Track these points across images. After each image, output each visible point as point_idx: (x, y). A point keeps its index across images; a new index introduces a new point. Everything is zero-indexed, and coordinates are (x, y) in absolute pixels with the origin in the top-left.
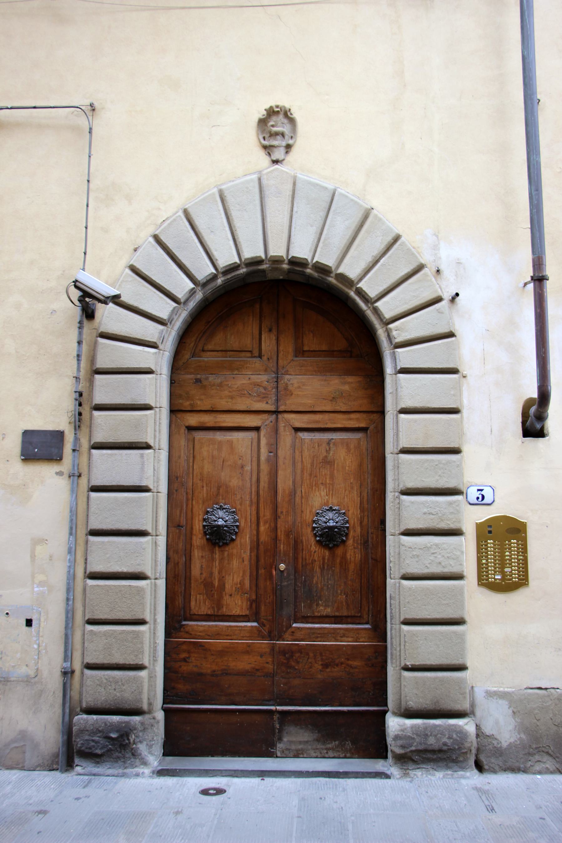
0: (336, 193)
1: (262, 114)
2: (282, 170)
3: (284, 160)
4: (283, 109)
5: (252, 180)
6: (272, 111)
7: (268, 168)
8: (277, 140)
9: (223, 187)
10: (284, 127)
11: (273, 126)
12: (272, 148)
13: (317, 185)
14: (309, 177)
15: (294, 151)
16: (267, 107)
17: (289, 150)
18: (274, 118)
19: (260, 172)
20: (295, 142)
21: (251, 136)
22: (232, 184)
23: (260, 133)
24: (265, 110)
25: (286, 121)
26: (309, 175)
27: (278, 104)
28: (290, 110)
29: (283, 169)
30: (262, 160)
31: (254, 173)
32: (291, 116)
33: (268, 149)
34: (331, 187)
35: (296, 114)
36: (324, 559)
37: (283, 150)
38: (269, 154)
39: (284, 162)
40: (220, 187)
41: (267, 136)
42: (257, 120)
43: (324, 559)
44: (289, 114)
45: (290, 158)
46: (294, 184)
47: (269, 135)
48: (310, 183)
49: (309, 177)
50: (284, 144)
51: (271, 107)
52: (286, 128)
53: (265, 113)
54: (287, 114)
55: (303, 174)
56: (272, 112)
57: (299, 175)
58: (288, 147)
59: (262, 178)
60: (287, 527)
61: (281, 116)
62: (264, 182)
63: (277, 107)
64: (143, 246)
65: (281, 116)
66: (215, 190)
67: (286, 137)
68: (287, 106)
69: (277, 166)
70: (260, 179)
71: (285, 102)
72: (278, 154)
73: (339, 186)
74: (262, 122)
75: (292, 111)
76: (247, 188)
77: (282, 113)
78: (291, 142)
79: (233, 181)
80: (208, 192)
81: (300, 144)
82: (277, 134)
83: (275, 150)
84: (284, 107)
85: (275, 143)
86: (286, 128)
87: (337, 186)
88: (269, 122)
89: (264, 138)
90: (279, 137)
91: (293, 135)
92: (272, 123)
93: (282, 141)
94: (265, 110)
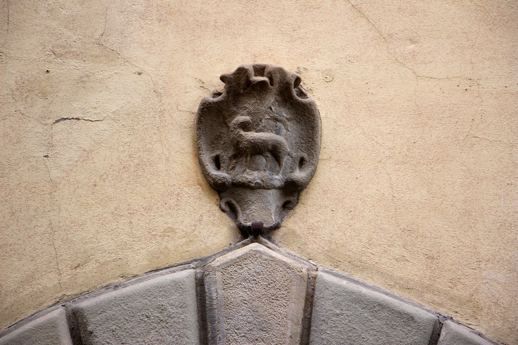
1: (213, 90)
3: (277, 227)
4: (277, 78)
5: (177, 285)
7: (228, 251)
8: (257, 169)
11: (245, 126)
12: (240, 191)
14: (357, 282)
16: (230, 69)
17: (291, 198)
18: (250, 104)
19: (202, 262)
20: (312, 175)
25: (284, 113)
26: (356, 277)
27: (260, 62)
28: (298, 80)
29: (274, 254)
31: (184, 265)
33: (228, 195)
35: (318, 94)
37: (273, 199)
38: (232, 211)
44: (294, 92)
49: (357, 282)
50: (278, 179)
51: (241, 71)
52: (285, 137)
53: (221, 86)
54: (288, 93)
55: (336, 270)
56: (242, 86)
58: (292, 193)
59: (207, 279)
61: (271, 99)
63: (260, 70)
65: (271, 99)
67: (286, 160)
68: (290, 69)
71: (284, 59)
74: (213, 117)
75: (304, 86)
77: (274, 89)
78: (299, 175)
82: (257, 149)
83: (251, 196)
84: (281, 71)
85: (253, 176)
86: (285, 137)
88: (234, 114)
89: (217, 162)
90: (262, 160)
91: (305, 155)
92: (241, 118)
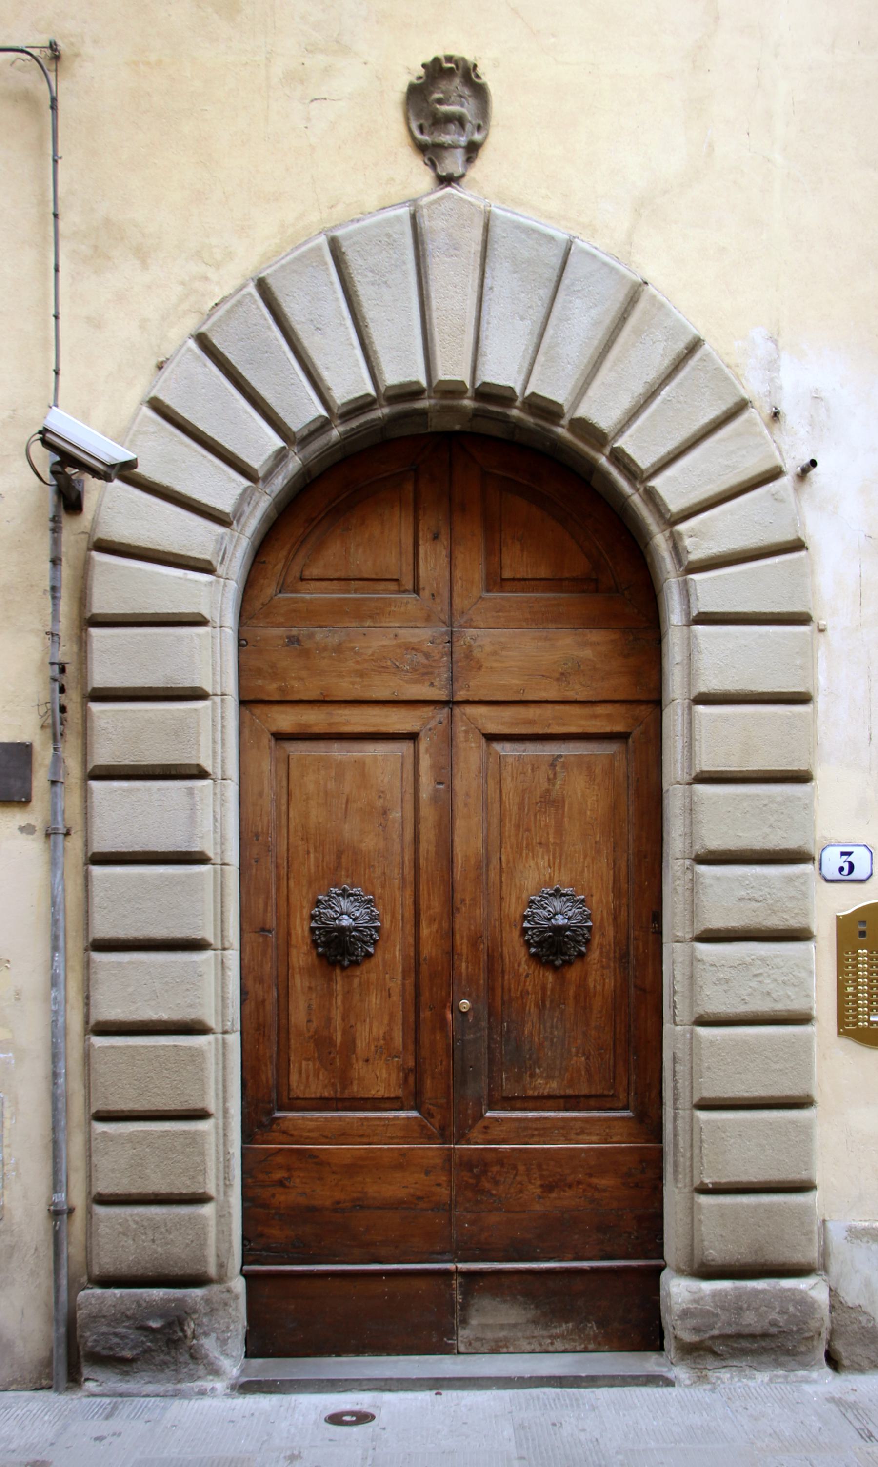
0: (573, 248)
1: (416, 74)
2: (461, 199)
3: (463, 176)
4: (461, 65)
5: (398, 219)
6: (437, 68)
8: (448, 133)
9: (338, 233)
10: (462, 106)
11: (440, 102)
13: (534, 231)
14: (517, 214)
15: (485, 155)
16: (429, 59)
17: (473, 155)
18: (443, 85)
19: (414, 202)
20: (486, 138)
21: (392, 125)
22: (356, 226)
23: (412, 118)
24: (424, 66)
25: (467, 92)
26: (516, 211)
28: (475, 66)
29: (462, 195)
30: (418, 177)
31: (402, 204)
32: (476, 80)
33: (430, 152)
34: (562, 236)
35: (488, 76)
37: (459, 155)
38: (433, 165)
39: (464, 181)
40: (331, 234)
41: (426, 124)
42: (405, 88)
45: (480, 171)
46: (487, 228)
47: (430, 122)
48: (518, 227)
49: (517, 214)
50: (463, 141)
51: (436, 60)
52: (467, 109)
53: (422, 72)
55: (503, 206)
56: (438, 71)
57: (493, 209)
58: (472, 150)
59: (417, 215)
60: (472, 928)
61: (457, 81)
62: (426, 223)
63: (449, 59)
64: (177, 360)
65: (457, 81)
66: (323, 240)
67: (468, 127)
68: (470, 58)
69: (448, 190)
70: (413, 217)
72: (453, 163)
73: (577, 234)
74: (418, 96)
75: (480, 71)
76: (388, 236)
77: (459, 73)
78: (477, 137)
79: (358, 221)
80: (306, 243)
81: (496, 141)
83: (446, 154)
84: (463, 59)
85: (446, 139)
86: (467, 109)
87: (574, 233)
88: (432, 93)
89: (421, 129)
90: (452, 127)
91: (481, 123)
92: (438, 95)
93: (460, 134)
94: (424, 66)
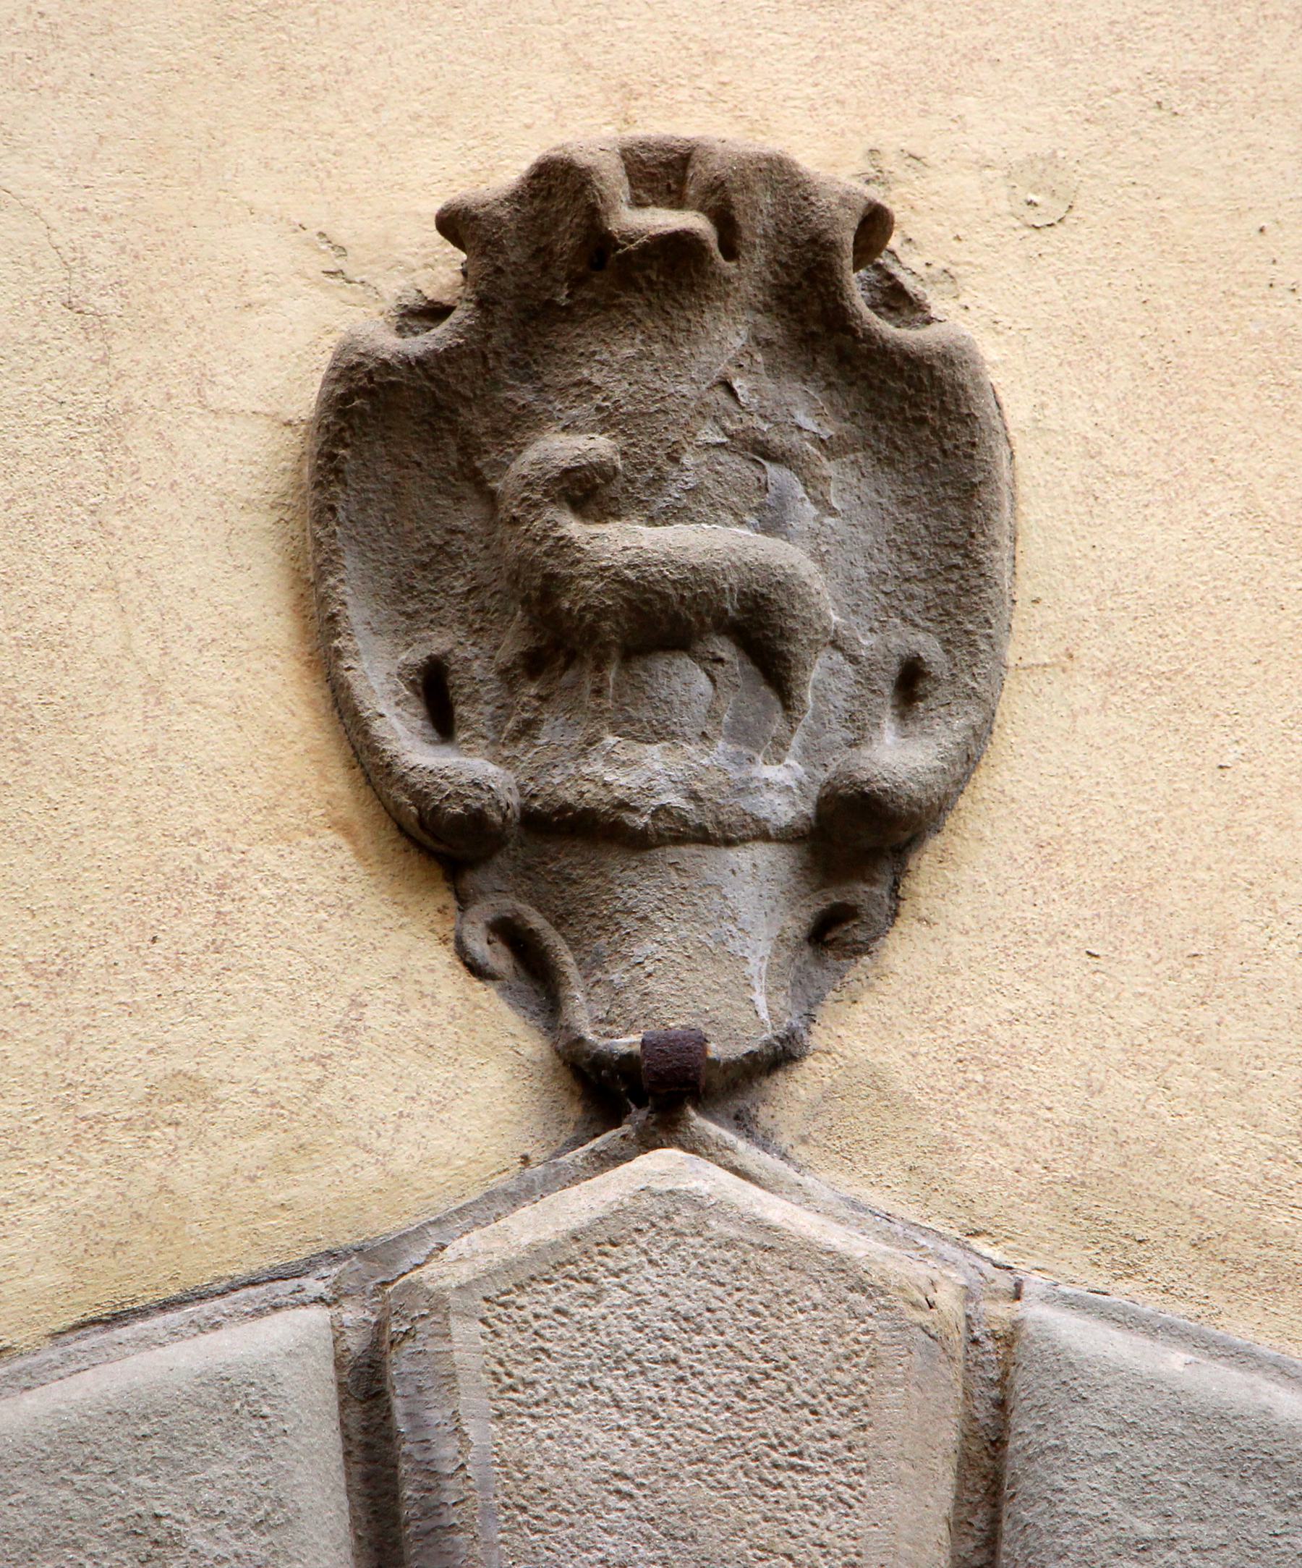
1: (397, 288)
2: (770, 1240)
3: (781, 1056)
4: (758, 216)
5: (236, 1402)
7: (515, 1198)
8: (660, 733)
11: (586, 491)
12: (569, 860)
14: (1242, 1357)
15: (962, 896)
16: (496, 172)
17: (858, 893)
18: (616, 362)
19: (371, 1265)
20: (969, 760)
21: (196, 678)
23: (357, 612)
24: (453, 224)
25: (805, 413)
26: (1238, 1330)
27: (664, 124)
28: (875, 223)
29: (775, 1210)
31: (272, 1283)
32: (886, 328)
33: (504, 876)
35: (980, 297)
36: (635, 810)
37: (753, 895)
38: (532, 971)
41: (476, 663)
43: (635, 810)
44: (856, 288)
49: (1242, 1357)
50: (781, 786)
51: (557, 182)
52: (811, 541)
53: (442, 269)
54: (826, 300)
55: (1123, 1292)
56: (560, 264)
58: (859, 855)
59: (400, 1365)
61: (728, 336)
63: (663, 171)
65: (728, 336)
67: (820, 676)
68: (831, 160)
71: (799, 114)
72: (707, 956)
74: (400, 440)
75: (909, 258)
77: (747, 275)
78: (898, 757)
81: (1060, 785)
82: (662, 620)
83: (639, 886)
84: (778, 174)
85: (641, 772)
86: (811, 541)
88: (521, 424)
89: (436, 696)
90: (686, 682)
91: (929, 647)
92: (561, 446)
93: (746, 735)
94: (453, 224)
